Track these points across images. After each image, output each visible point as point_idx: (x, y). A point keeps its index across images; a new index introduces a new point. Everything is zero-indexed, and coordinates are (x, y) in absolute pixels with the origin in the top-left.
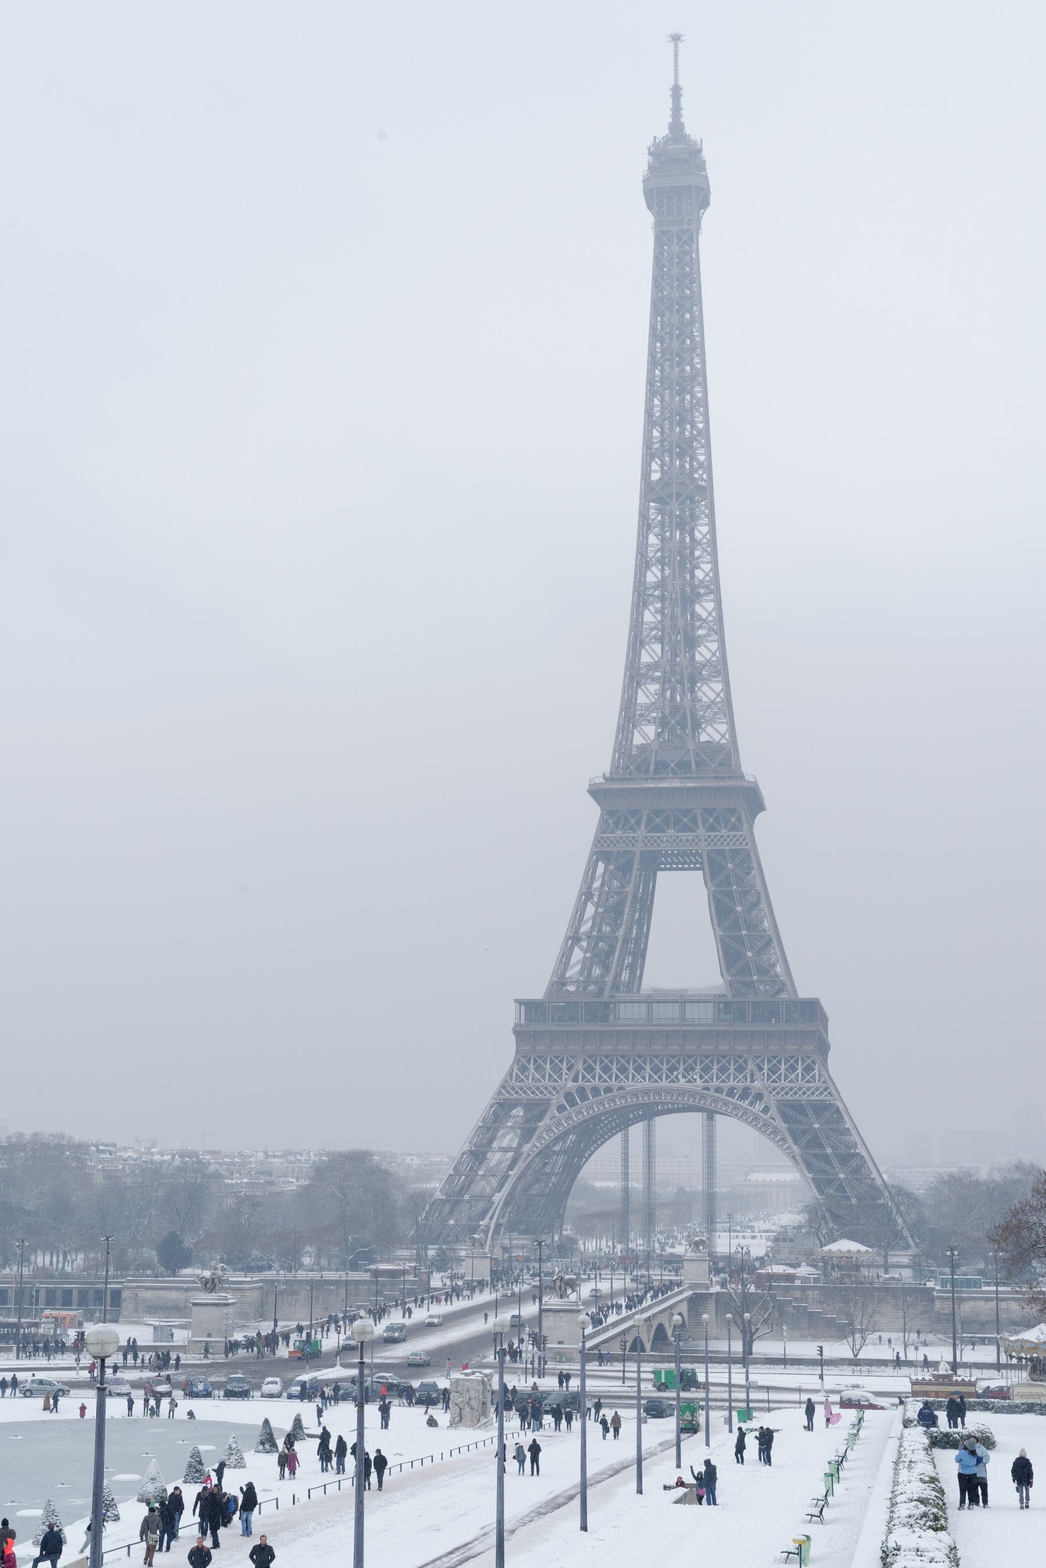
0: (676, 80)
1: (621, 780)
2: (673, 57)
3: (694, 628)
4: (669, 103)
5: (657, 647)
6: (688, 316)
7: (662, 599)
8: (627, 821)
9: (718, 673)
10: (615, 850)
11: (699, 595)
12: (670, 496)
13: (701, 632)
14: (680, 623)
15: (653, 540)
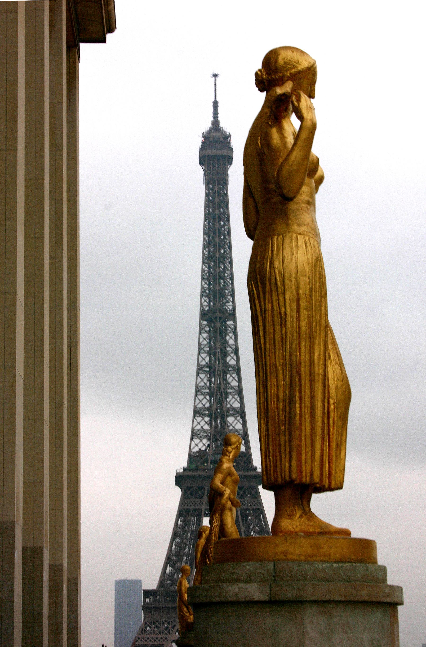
0: (215, 98)
1: (194, 470)
2: (214, 86)
3: (226, 388)
4: (212, 110)
5: (208, 397)
6: (222, 223)
7: (210, 373)
8: (197, 493)
9: (238, 413)
10: (191, 508)
11: (229, 371)
12: (216, 318)
13: (229, 391)
14: (222, 387)
15: (205, 343)
